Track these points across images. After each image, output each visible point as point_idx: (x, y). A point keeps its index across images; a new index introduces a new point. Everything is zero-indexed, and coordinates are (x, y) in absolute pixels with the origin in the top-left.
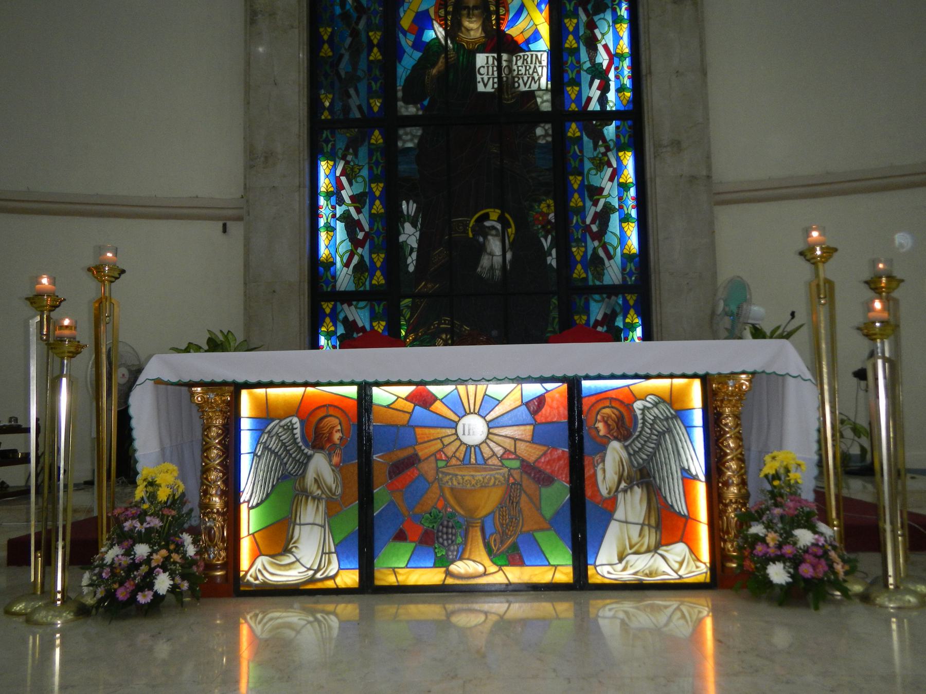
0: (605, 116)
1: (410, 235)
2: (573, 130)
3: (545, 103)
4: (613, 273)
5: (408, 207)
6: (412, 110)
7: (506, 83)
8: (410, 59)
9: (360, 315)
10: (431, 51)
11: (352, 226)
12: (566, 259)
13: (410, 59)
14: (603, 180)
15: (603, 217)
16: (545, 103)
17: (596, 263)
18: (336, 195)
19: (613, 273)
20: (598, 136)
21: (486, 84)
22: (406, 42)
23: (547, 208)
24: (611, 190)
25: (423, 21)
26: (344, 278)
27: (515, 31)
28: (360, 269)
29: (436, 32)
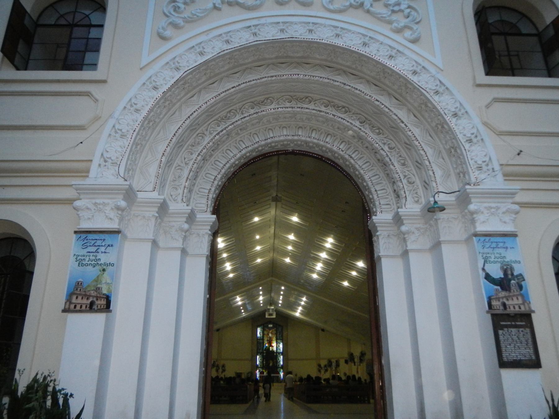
0: (280, 353)
1: (264, 362)
2: (277, 354)
3: (275, 352)
4: (280, 366)
5: (264, 360)
6: (265, 352)
7: (272, 350)
8: (264, 348)
9: (260, 369)
10: (267, 347)
11: (260, 361)
12: (277, 365)
13: (264, 348)
14: (280, 358)
15: (280, 361)
16: (275, 352)
17: (279, 365)
18: (259, 359)
19: (280, 366)
20: (279, 354)
21: (271, 350)
22: (264, 346)
23: (275, 361)
24: (280, 359)
25: (266, 344)
26: (259, 366)
27: (273, 345)
28: (261, 365)
29: (267, 345)
